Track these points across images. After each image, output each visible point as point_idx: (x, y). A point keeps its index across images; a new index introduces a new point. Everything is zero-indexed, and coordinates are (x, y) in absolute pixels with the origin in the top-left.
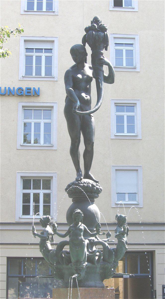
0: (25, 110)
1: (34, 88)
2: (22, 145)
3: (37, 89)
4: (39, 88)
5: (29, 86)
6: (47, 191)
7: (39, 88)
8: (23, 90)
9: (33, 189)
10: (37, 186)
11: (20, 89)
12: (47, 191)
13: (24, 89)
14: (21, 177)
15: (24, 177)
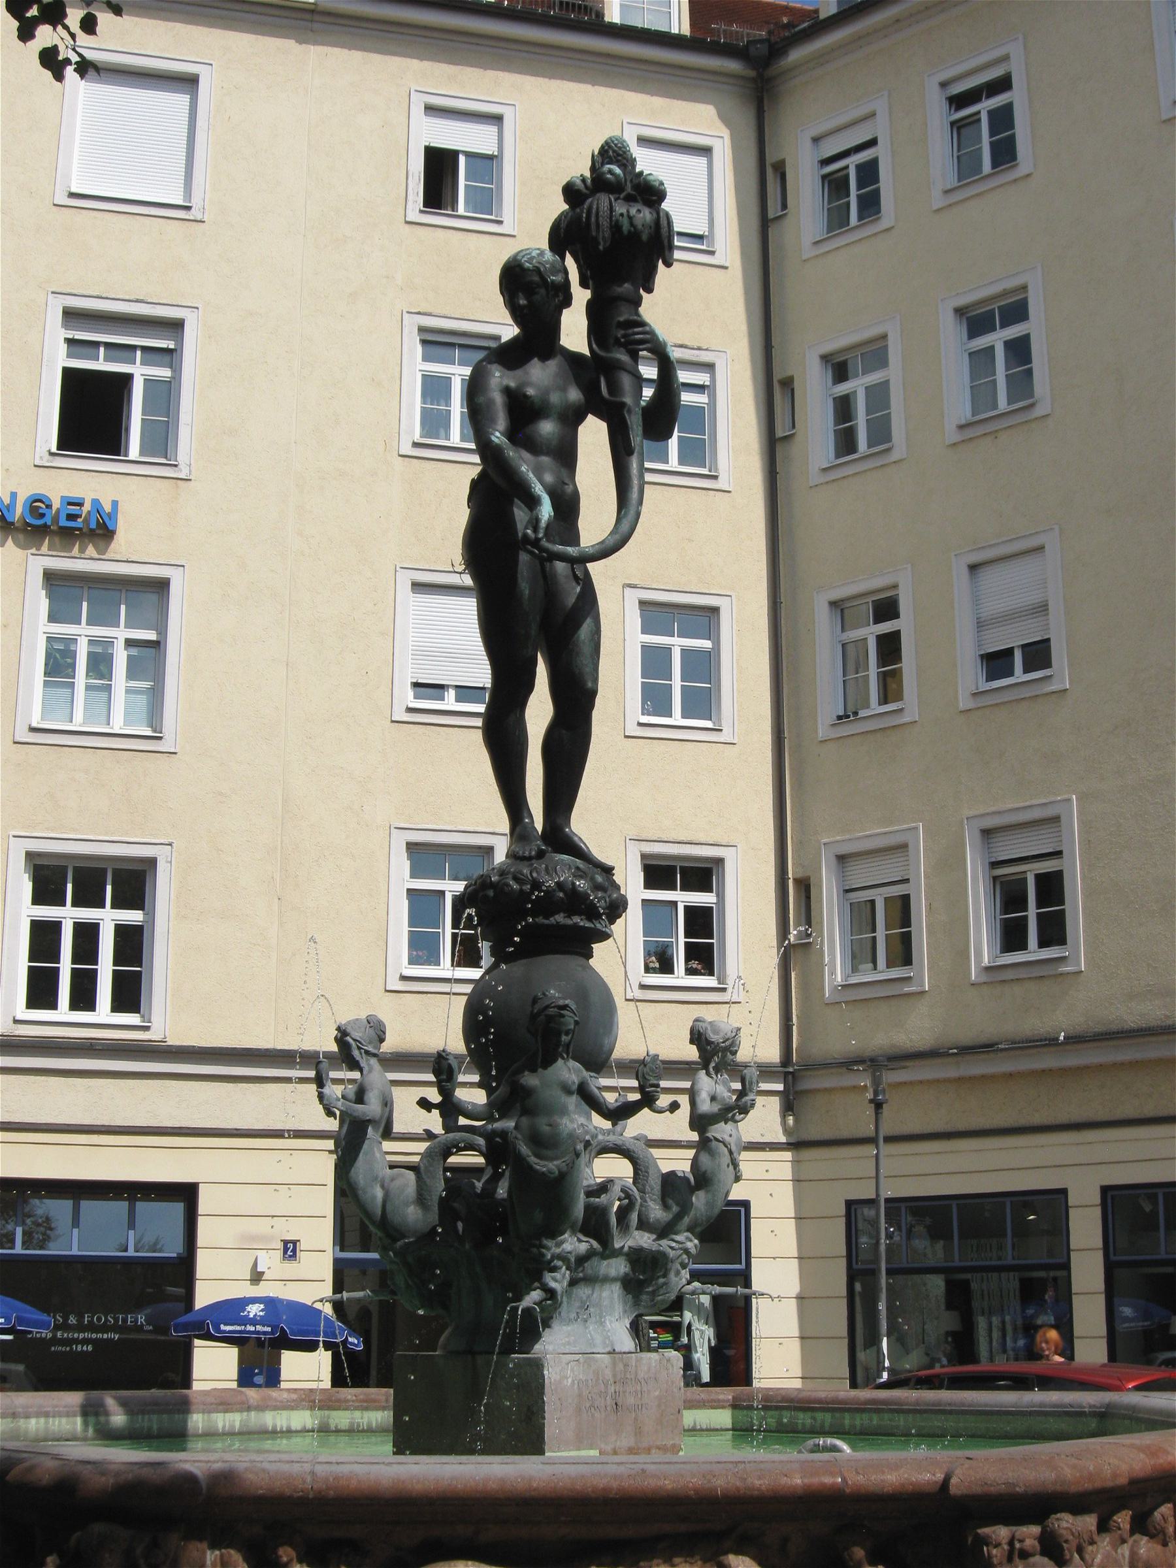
0: (51, 585)
1: (96, 502)
2: (34, 725)
3: (108, 508)
4: (115, 504)
5: (75, 494)
6: (133, 916)
7: (115, 504)
8: (49, 506)
9: (76, 903)
10: (89, 896)
11: (37, 505)
12: (133, 916)
13: (56, 504)
14: (30, 855)
15: (40, 855)
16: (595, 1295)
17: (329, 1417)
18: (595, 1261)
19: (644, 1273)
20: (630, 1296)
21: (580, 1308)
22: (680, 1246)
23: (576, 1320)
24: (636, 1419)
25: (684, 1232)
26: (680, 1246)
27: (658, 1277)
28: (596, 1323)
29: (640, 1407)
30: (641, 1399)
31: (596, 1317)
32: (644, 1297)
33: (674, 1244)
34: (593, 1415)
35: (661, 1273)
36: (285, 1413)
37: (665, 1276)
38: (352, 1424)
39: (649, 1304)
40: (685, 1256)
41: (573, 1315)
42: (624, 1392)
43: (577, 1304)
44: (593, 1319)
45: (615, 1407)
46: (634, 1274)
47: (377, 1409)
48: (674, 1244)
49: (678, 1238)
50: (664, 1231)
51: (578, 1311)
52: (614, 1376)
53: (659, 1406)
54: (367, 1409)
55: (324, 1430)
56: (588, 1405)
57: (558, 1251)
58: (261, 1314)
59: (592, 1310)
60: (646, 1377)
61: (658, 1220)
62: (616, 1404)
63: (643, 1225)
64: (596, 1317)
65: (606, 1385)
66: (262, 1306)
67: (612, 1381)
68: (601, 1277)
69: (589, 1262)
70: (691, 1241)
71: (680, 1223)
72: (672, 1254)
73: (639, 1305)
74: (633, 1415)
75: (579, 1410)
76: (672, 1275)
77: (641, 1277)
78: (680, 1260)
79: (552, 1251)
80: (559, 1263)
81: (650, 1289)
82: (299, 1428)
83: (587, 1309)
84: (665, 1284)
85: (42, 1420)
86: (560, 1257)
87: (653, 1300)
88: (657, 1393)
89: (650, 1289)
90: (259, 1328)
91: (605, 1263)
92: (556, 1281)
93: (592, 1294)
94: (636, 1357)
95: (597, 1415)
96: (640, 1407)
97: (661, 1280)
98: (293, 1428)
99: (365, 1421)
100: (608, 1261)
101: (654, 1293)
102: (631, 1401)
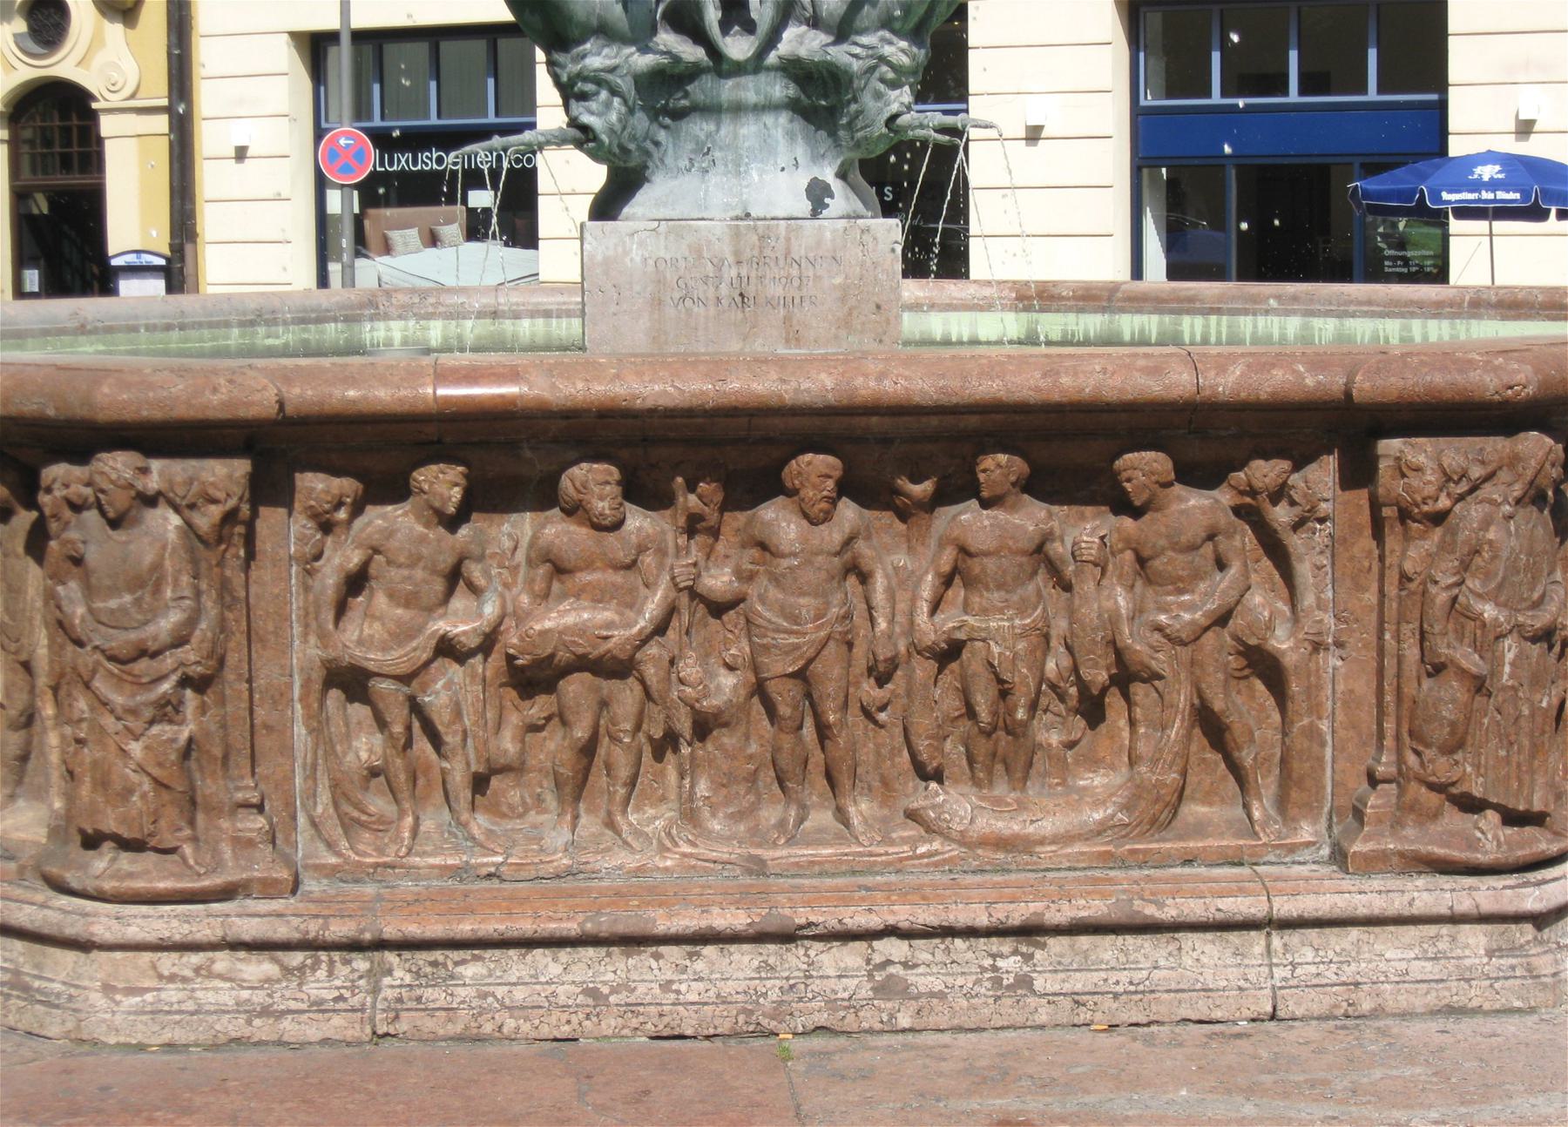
16: (723, 132)
17: (1037, 322)
18: (707, 81)
19: (826, 97)
20: (822, 134)
21: (694, 151)
22: (870, 52)
23: (689, 170)
24: (787, 320)
25: (878, 29)
26: (870, 52)
27: (849, 102)
28: (725, 174)
29: (797, 301)
30: (799, 288)
31: (726, 166)
32: (841, 133)
33: (857, 50)
34: (689, 312)
35: (850, 96)
36: (966, 316)
37: (855, 100)
38: (1065, 333)
39: (851, 144)
40: (884, 68)
41: (684, 163)
42: (761, 278)
43: (690, 146)
44: (720, 168)
45: (738, 299)
46: (809, 97)
47: (1095, 311)
48: (857, 50)
49: (865, 40)
50: (843, 31)
51: (693, 156)
52: (737, 253)
53: (843, 299)
54: (1081, 310)
55: (1031, 340)
56: (677, 295)
57: (574, 68)
58: (1501, 176)
59: (717, 154)
60: (811, 255)
61: (831, 14)
62: (741, 295)
63: (815, 22)
64: (726, 166)
65: (719, 267)
66: (1498, 168)
67: (731, 259)
68: (726, 105)
69: (696, 83)
70: (890, 43)
71: (859, 17)
72: (856, 66)
73: (840, 145)
74: (782, 312)
75: (657, 303)
76: (867, 99)
77: (823, 103)
78: (877, 74)
79: (568, 70)
80: (590, 87)
81: (844, 121)
82: (993, 338)
83: (707, 153)
84: (859, 113)
85: (540, 322)
86: (581, 76)
87: (852, 138)
88: (838, 280)
89: (844, 121)
90: (1501, 195)
91: (730, 83)
92: (592, 113)
93: (718, 131)
94: (788, 227)
95: (698, 310)
96: (797, 301)
97: (853, 107)
98: (983, 338)
99: (1081, 328)
100: (738, 80)
101: (850, 126)
102: (776, 291)
